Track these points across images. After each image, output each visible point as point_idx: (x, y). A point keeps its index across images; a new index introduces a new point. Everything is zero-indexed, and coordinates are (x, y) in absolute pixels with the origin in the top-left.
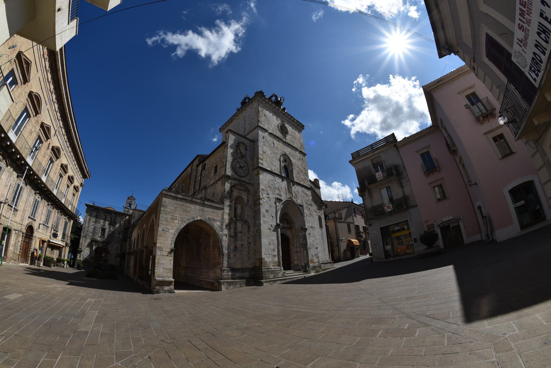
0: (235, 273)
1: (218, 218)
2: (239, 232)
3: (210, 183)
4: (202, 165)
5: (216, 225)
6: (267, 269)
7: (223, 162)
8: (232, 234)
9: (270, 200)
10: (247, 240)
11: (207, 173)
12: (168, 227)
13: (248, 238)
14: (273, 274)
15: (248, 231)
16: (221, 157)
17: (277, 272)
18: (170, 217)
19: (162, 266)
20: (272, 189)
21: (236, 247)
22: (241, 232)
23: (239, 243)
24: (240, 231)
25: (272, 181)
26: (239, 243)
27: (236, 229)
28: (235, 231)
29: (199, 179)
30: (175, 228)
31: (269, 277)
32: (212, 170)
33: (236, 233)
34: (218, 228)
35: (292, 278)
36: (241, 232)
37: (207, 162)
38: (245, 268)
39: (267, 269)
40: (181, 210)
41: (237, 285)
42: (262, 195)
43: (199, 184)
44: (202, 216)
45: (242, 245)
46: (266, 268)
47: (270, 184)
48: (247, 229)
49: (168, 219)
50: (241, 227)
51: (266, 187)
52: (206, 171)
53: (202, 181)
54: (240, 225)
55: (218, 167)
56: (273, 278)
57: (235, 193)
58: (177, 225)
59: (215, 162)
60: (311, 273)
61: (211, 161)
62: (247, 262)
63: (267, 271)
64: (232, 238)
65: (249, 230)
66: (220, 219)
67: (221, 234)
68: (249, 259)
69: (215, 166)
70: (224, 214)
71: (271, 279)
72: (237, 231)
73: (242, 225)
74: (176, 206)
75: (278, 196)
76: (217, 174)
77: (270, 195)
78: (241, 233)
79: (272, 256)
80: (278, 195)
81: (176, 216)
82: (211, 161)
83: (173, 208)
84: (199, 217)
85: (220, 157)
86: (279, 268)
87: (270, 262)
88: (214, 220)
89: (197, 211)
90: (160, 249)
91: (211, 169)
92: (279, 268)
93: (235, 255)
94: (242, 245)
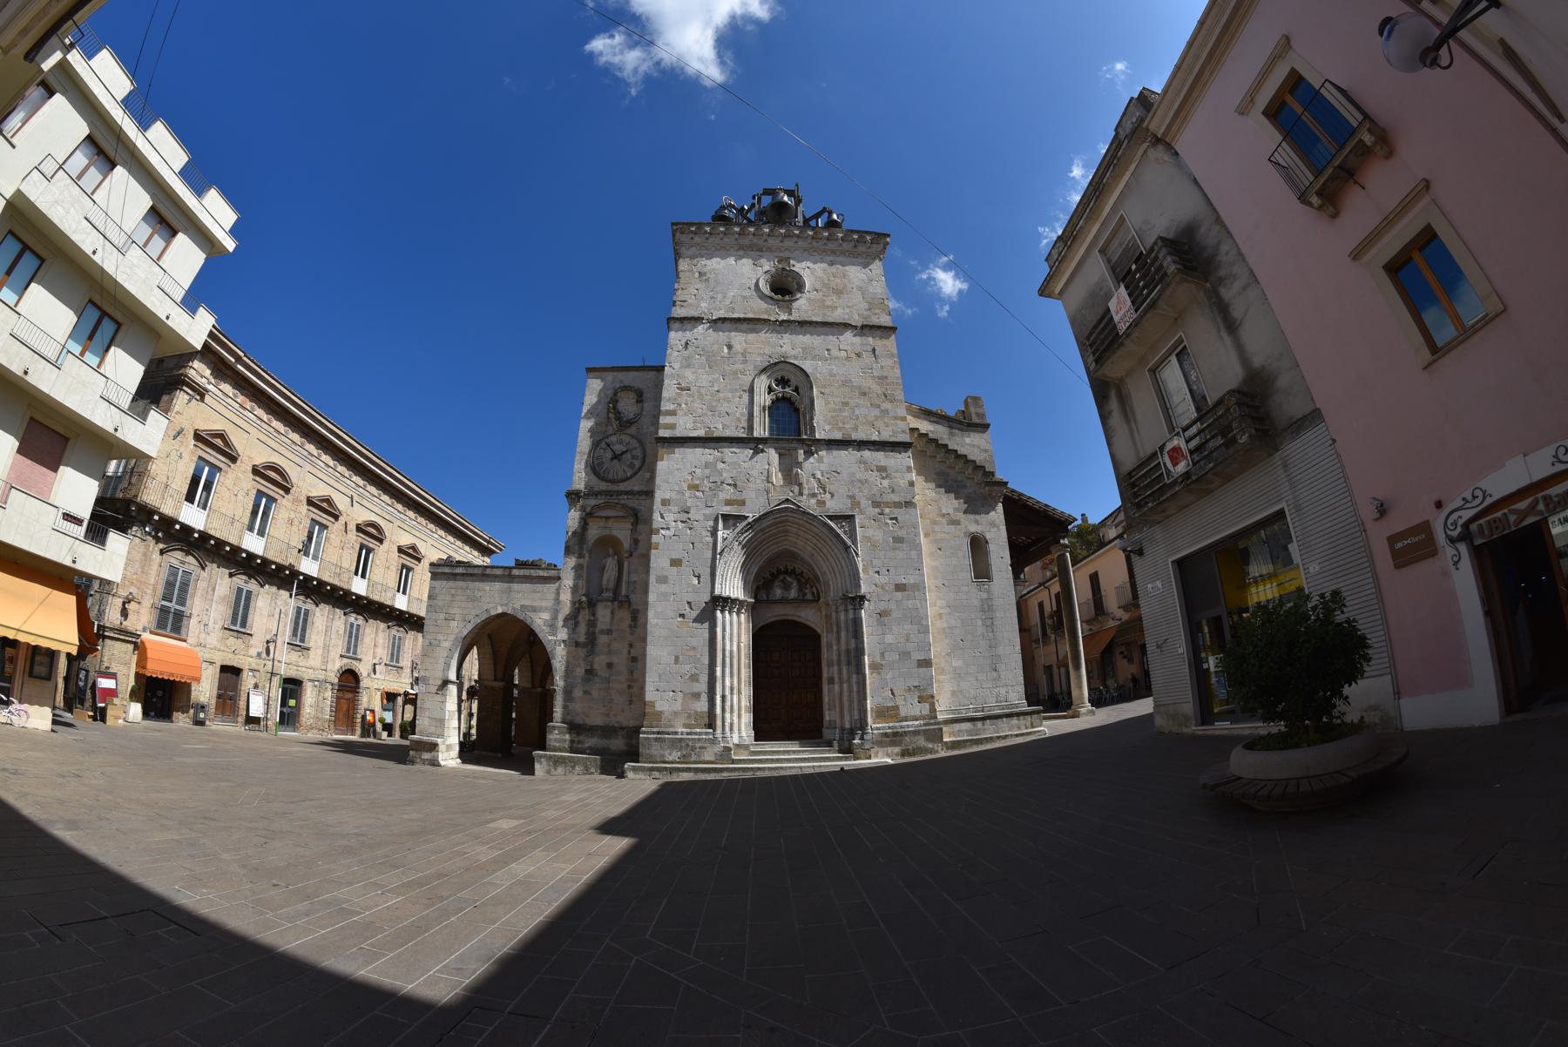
0: (581, 738)
1: (544, 604)
2: (602, 632)
5: (539, 621)
6: (658, 733)
8: (582, 639)
9: (691, 529)
10: (625, 652)
12: (440, 637)
13: (631, 645)
14: (681, 749)
15: (630, 626)
17: (698, 745)
18: (442, 616)
19: (427, 714)
20: (703, 492)
21: (590, 672)
22: (609, 632)
23: (600, 661)
24: (605, 627)
25: (707, 465)
26: (600, 661)
27: (592, 624)
28: (591, 629)
30: (452, 637)
31: (663, 756)
33: (594, 633)
34: (544, 628)
35: (752, 768)
36: (609, 632)
38: (616, 725)
39: (658, 733)
40: (463, 598)
41: (577, 768)
42: (662, 517)
44: (506, 605)
45: (610, 665)
46: (655, 730)
47: (699, 479)
48: (628, 621)
49: (439, 622)
50: (608, 619)
51: (681, 492)
54: (608, 612)
56: (678, 763)
57: (594, 532)
58: (456, 631)
60: (870, 758)
62: (623, 712)
63: (656, 739)
64: (580, 649)
65: (633, 623)
66: (549, 604)
67: (550, 641)
68: (631, 702)
70: (561, 591)
71: (672, 763)
72: (597, 630)
73: (613, 613)
74: (453, 591)
75: (727, 510)
77: (692, 511)
78: (608, 634)
79: (685, 695)
80: (728, 503)
81: (453, 612)
83: (448, 598)
84: (499, 607)
86: (707, 734)
87: (675, 713)
88: (535, 610)
89: (496, 595)
90: (424, 680)
92: (707, 734)
93: (586, 692)
94: (610, 665)
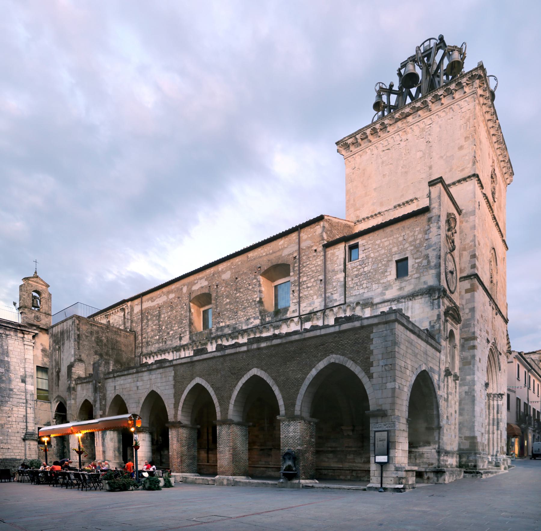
3: (383, 294)
4: (345, 246)
7: (427, 257)
11: (366, 269)
16: (418, 242)
29: (342, 279)
32: (386, 266)
37: (361, 241)
43: (341, 290)
52: (363, 263)
53: (350, 284)
55: (410, 262)
59: (395, 249)
61: (378, 242)
69: (397, 259)
76: (406, 278)
82: (378, 242)
85: (415, 240)
91: (383, 263)
